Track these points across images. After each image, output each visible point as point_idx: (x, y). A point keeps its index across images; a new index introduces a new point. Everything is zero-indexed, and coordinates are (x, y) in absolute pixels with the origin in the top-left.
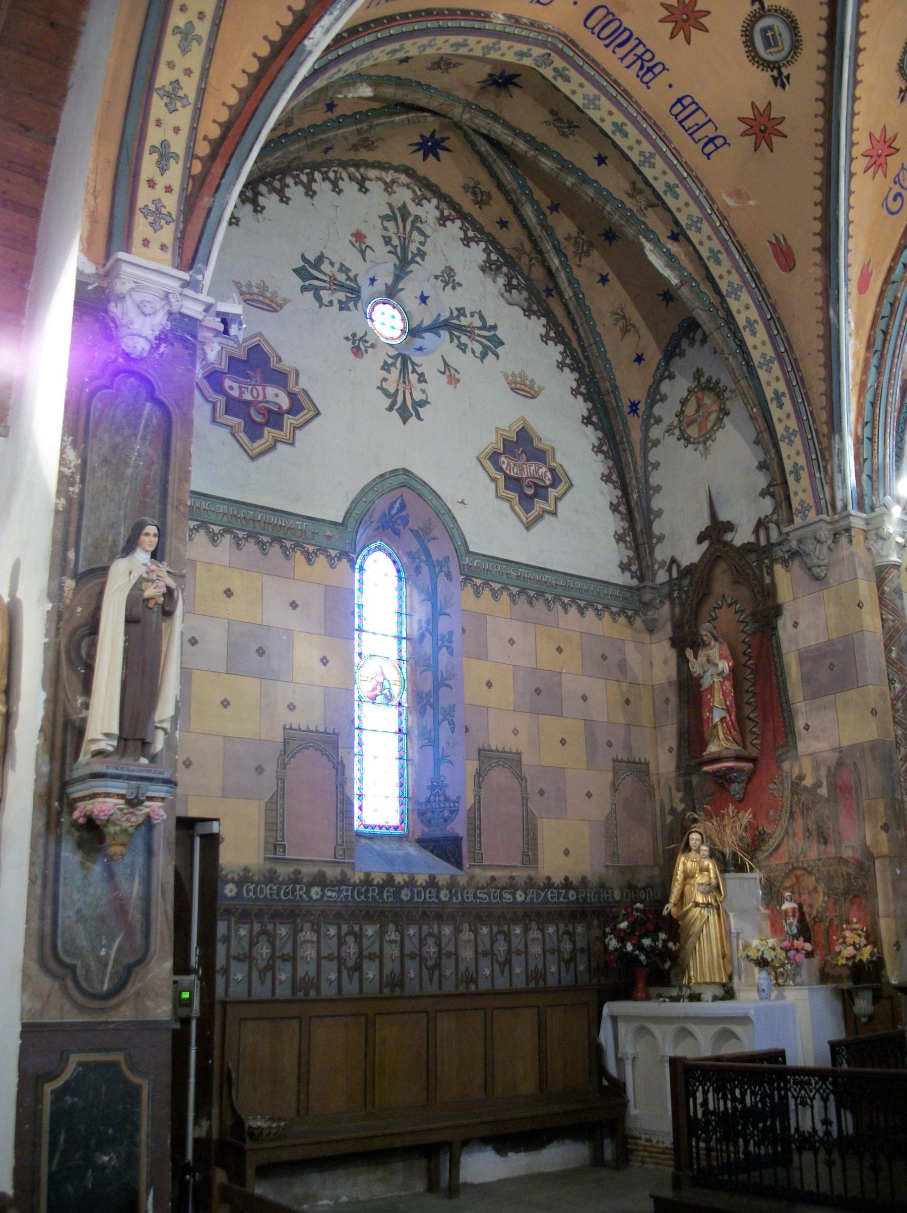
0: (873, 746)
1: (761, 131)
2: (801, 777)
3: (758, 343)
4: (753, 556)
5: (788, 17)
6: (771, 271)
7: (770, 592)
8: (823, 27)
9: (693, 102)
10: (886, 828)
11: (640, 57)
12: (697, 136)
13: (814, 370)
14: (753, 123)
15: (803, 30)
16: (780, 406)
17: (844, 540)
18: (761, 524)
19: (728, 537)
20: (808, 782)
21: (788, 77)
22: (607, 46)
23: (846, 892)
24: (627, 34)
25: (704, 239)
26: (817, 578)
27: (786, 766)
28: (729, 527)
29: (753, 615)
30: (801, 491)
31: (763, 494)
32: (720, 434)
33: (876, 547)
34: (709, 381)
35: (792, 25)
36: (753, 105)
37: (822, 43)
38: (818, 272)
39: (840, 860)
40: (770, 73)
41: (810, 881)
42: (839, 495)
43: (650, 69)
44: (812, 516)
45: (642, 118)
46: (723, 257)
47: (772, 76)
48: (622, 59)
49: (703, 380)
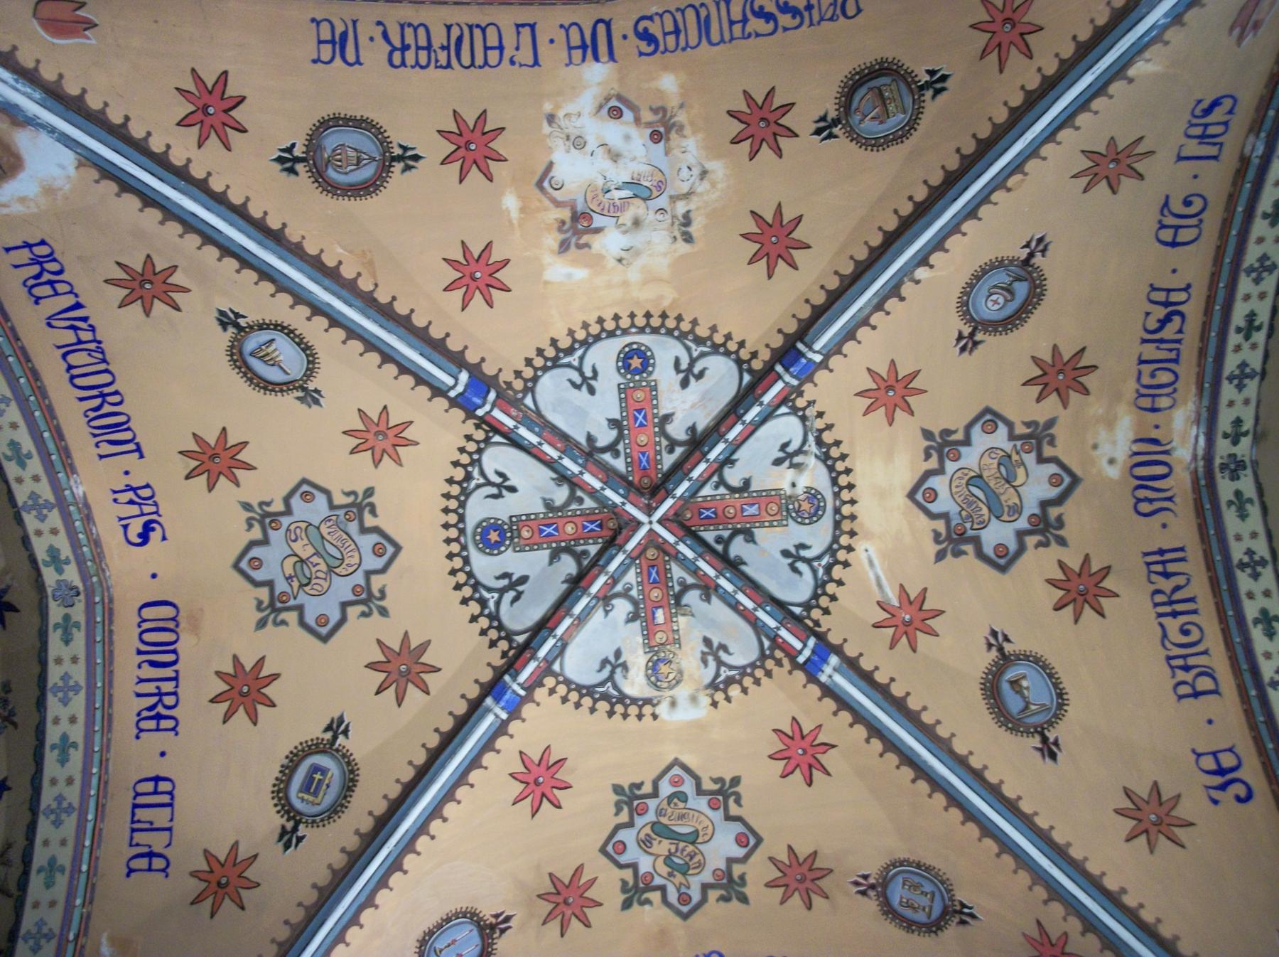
1: (219, 884)
5: (352, 772)
8: (380, 808)
9: (170, 793)
11: (160, 694)
12: (139, 837)
14: (216, 867)
21: (300, 839)
22: (139, 652)
24: (171, 657)
35: (350, 783)
36: (235, 846)
37: (367, 824)
40: (283, 821)
43: (159, 717)
45: (98, 757)
47: (283, 827)
48: (141, 681)
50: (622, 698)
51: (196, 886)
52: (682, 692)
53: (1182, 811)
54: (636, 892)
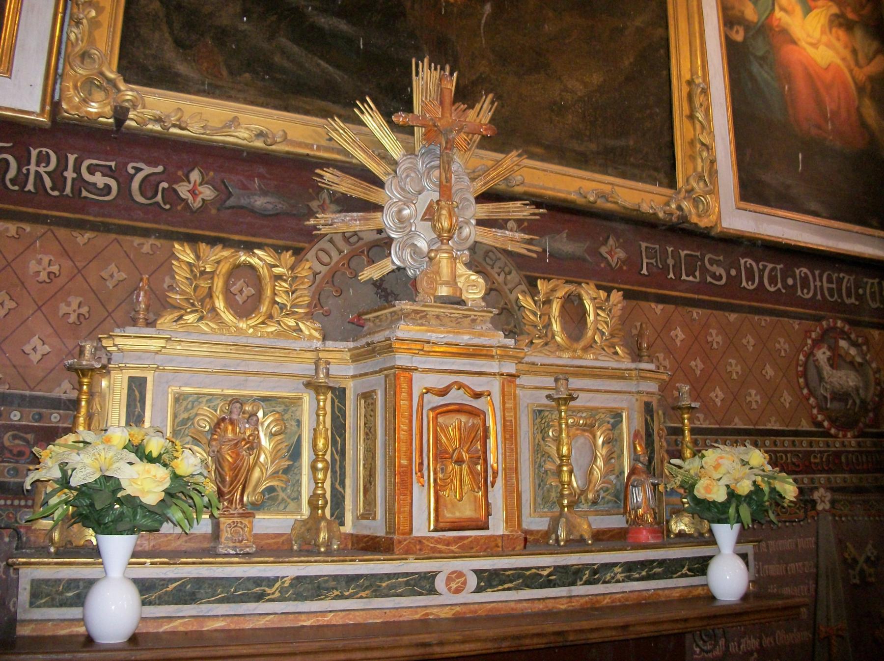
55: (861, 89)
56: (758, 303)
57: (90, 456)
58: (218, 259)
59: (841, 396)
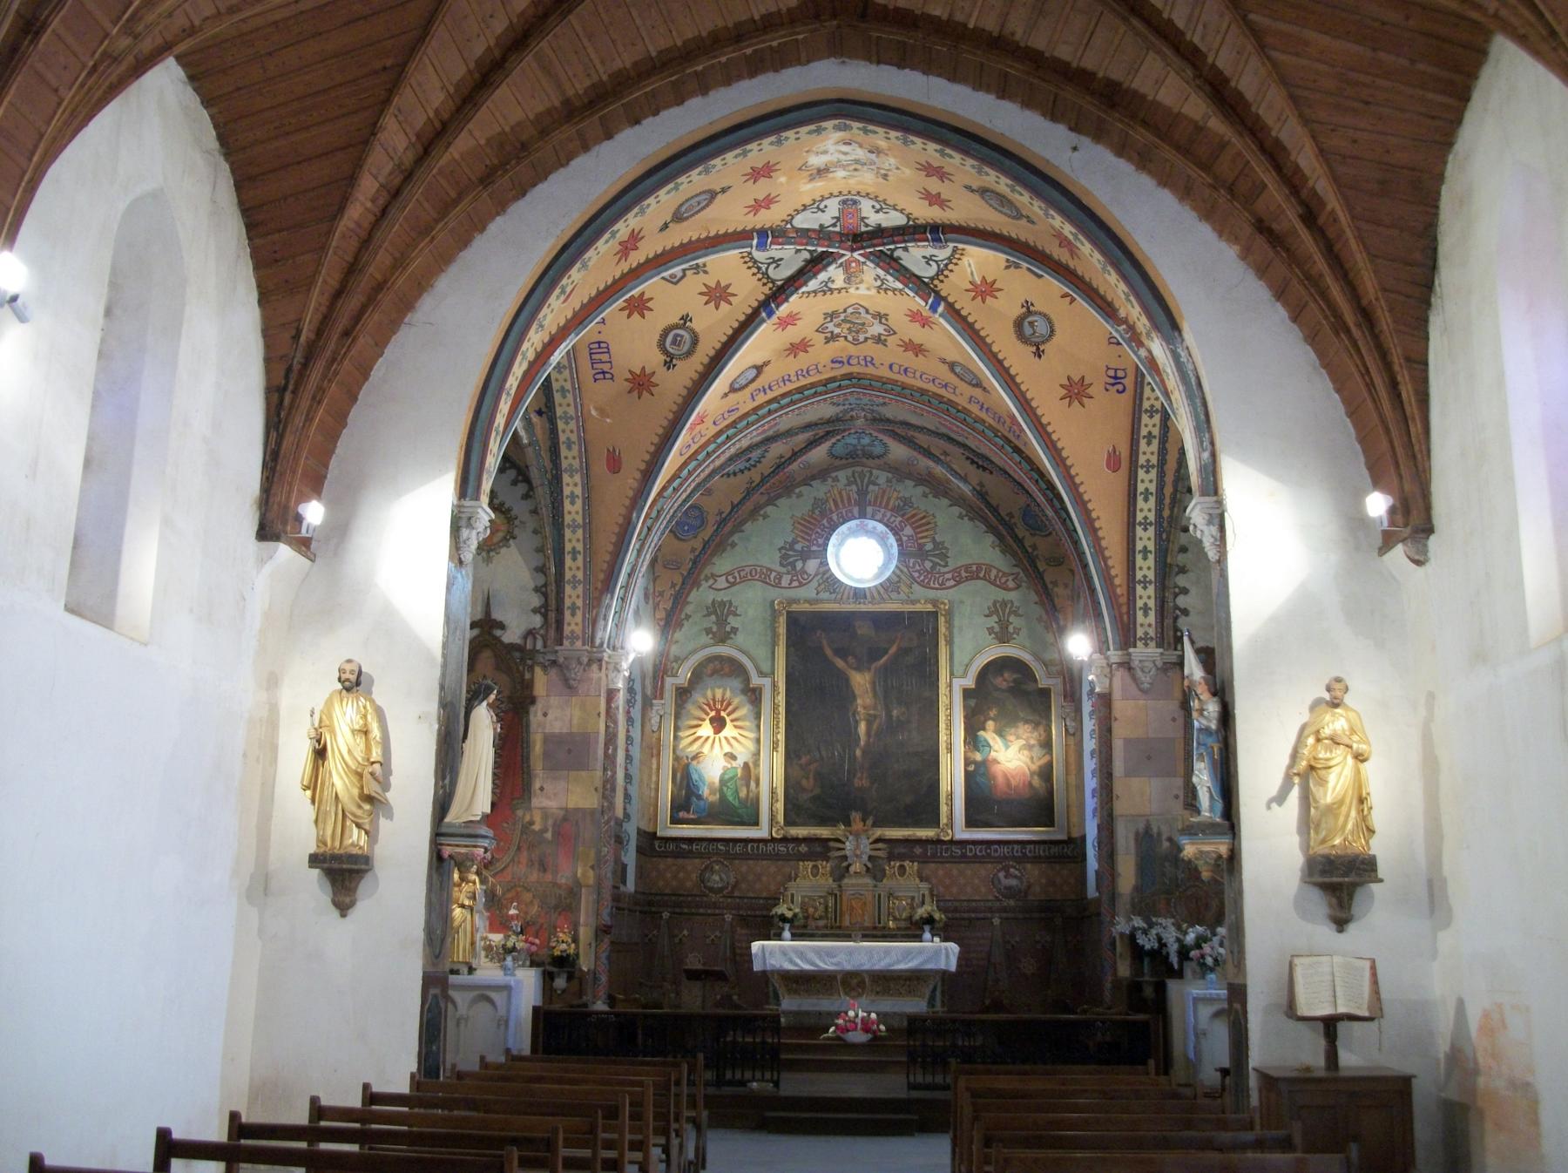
0: (593, 812)
2: (532, 823)
3: (573, 511)
4: (517, 654)
6: (600, 467)
7: (529, 685)
8: (712, 353)
10: (592, 867)
13: (605, 544)
15: (700, 347)
16: (574, 559)
17: (595, 667)
18: (530, 633)
19: (498, 633)
20: (537, 827)
23: (556, 907)
25: (566, 431)
26: (570, 687)
27: (520, 813)
28: (502, 626)
29: (510, 698)
30: (573, 623)
31: (535, 611)
32: (504, 550)
33: (612, 675)
34: (502, 504)
35: (695, 341)
37: (706, 360)
38: (635, 485)
39: (555, 884)
41: (527, 896)
42: (599, 635)
44: (579, 644)
46: (575, 448)
49: (496, 501)
50: (831, 290)
51: (628, 385)
52: (862, 286)
53: (1090, 391)
54: (833, 337)
55: (1032, 774)
56: (976, 859)
57: (782, 909)
58: (810, 864)
59: (1008, 888)
